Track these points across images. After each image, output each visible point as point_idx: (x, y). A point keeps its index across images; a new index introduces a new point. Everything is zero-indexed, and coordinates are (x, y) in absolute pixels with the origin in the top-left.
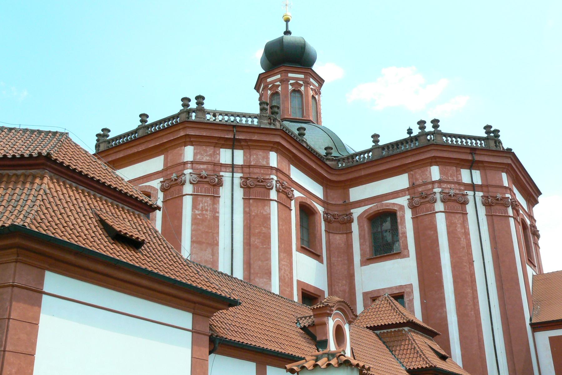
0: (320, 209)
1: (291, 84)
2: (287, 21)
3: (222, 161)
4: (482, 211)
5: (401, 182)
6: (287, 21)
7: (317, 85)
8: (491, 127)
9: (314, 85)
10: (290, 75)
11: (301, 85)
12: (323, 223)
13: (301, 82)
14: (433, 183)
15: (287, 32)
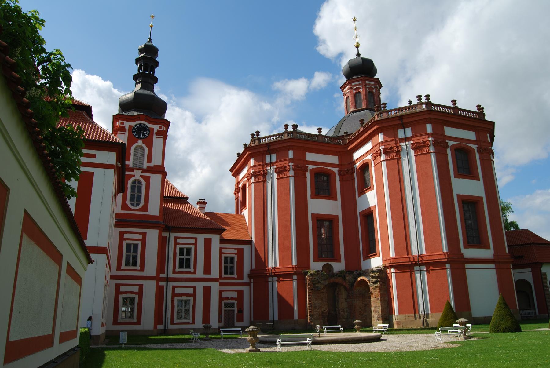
0: (335, 170)
1: (355, 90)
2: (357, 47)
3: (267, 162)
4: (412, 152)
5: (368, 146)
6: (357, 47)
7: (373, 83)
8: (421, 96)
9: (369, 84)
10: (353, 84)
11: (360, 88)
12: (338, 178)
13: (360, 87)
14: (379, 143)
15: (358, 55)
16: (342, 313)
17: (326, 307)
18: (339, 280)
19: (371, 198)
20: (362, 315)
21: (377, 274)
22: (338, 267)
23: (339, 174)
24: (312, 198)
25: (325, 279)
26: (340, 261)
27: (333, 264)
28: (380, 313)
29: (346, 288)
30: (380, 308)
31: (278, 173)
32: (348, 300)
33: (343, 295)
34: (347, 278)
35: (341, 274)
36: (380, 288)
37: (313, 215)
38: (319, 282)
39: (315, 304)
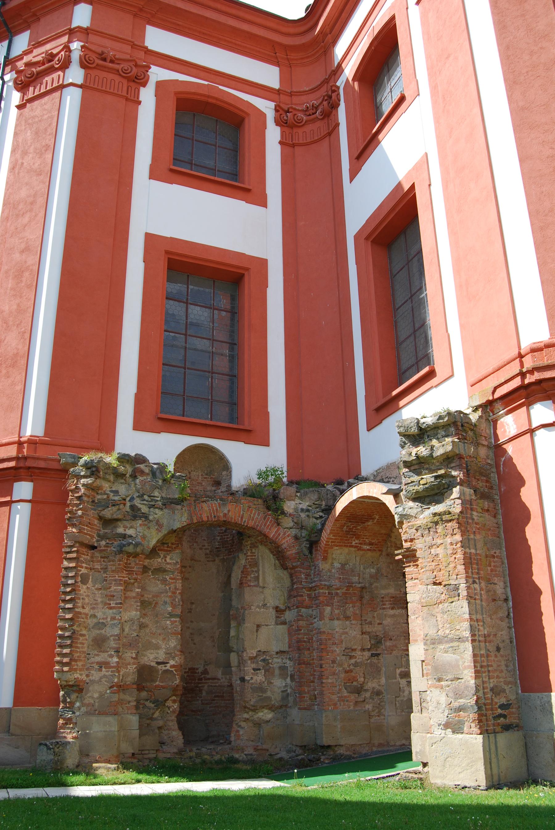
0: (266, 107)
12: (273, 134)
16: (260, 678)
17: (173, 643)
18: (251, 515)
19: (407, 147)
20: (359, 690)
21: (442, 446)
22: (247, 462)
23: (278, 122)
24: (154, 175)
25: (169, 503)
26: (265, 442)
27: (231, 449)
28: (469, 678)
29: (279, 553)
30: (468, 649)
31: (22, 86)
32: (289, 616)
33: (266, 589)
34: (289, 506)
35: (267, 495)
36: (464, 522)
37: (151, 240)
38: (135, 514)
39: (101, 625)
